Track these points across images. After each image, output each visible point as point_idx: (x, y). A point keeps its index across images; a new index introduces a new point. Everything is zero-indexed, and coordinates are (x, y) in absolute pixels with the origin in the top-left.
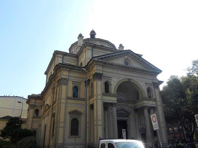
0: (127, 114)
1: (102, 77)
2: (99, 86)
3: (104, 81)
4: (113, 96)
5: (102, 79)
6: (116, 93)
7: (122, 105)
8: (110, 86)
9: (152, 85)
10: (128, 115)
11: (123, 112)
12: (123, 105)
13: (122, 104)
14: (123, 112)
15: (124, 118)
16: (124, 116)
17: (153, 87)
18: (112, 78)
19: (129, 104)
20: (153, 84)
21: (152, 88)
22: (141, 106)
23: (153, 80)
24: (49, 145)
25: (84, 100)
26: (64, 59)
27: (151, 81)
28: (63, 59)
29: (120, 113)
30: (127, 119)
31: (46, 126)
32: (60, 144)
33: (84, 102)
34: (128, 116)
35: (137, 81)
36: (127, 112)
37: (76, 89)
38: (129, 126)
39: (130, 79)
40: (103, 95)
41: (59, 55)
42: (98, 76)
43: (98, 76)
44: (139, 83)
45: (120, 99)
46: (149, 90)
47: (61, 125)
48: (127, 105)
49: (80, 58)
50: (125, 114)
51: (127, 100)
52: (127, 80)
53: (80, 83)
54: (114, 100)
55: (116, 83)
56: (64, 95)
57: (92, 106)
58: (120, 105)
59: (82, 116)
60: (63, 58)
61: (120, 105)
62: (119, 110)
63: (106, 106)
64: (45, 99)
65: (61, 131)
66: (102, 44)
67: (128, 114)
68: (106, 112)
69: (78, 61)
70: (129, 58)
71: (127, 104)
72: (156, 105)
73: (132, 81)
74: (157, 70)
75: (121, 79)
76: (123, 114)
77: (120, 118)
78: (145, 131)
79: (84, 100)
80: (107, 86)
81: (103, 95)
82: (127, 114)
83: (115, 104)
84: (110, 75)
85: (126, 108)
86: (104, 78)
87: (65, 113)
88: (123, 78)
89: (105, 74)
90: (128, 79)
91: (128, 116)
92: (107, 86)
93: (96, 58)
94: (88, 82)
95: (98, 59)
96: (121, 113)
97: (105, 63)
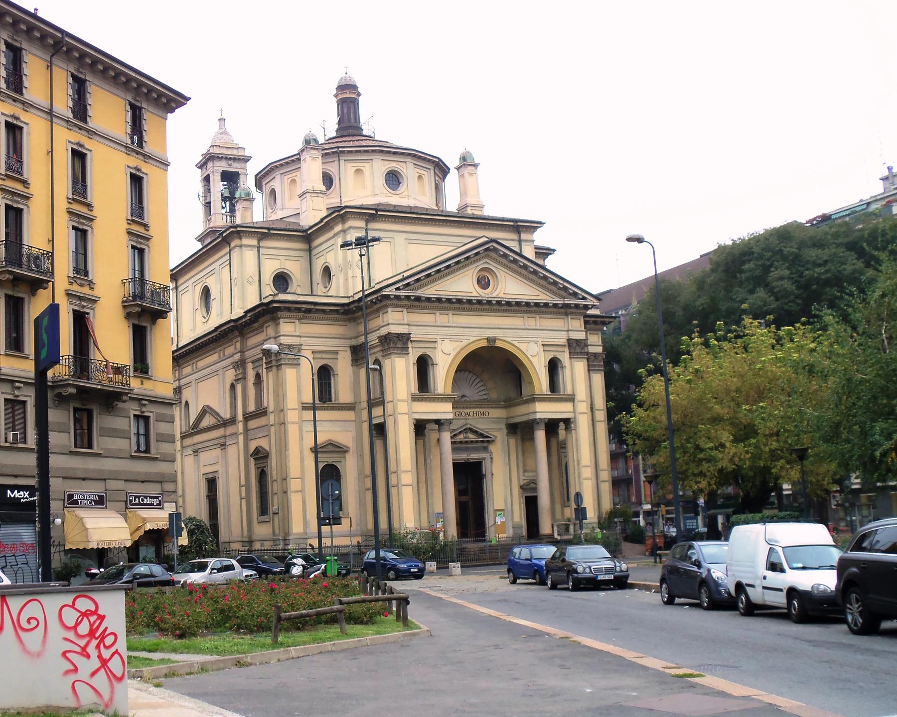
0: (482, 442)
1: (410, 345)
2: (400, 372)
3: (414, 353)
5: (410, 349)
6: (449, 391)
8: (431, 367)
9: (567, 350)
12: (471, 414)
13: (468, 411)
14: (472, 437)
15: (474, 456)
16: (476, 450)
18: (439, 341)
19: (490, 410)
20: (570, 346)
21: (564, 357)
22: (525, 418)
23: (568, 331)
24: (250, 537)
25: (350, 407)
26: (262, 251)
27: (564, 335)
28: (259, 251)
29: (461, 442)
30: (484, 459)
31: (212, 483)
32: (297, 534)
33: (350, 415)
34: (485, 449)
35: (516, 343)
36: (482, 435)
37: (324, 374)
38: (488, 476)
39: (494, 340)
40: (414, 398)
41: (245, 241)
42: (397, 343)
43: (397, 343)
44: (523, 347)
45: (463, 396)
46: (553, 366)
47: (294, 485)
48: (484, 414)
49: (318, 246)
50: (477, 442)
51: (485, 397)
52: (485, 344)
53: (336, 352)
54: (444, 410)
55: (451, 357)
56: (292, 401)
57: (379, 430)
59: (347, 455)
60: (259, 247)
61: (461, 414)
62: (460, 432)
63: (420, 427)
64: (183, 382)
65: (295, 501)
66: (394, 164)
67: (488, 441)
68: (420, 442)
69: (310, 254)
70: (492, 265)
71: (485, 410)
72: (574, 412)
73: (499, 344)
74: (584, 298)
75: (465, 342)
76: (472, 442)
77: (463, 456)
78: (535, 489)
79: (350, 407)
80: (423, 365)
81: (414, 398)
82: (485, 441)
83: (449, 422)
85: (480, 425)
86: (414, 344)
87: (301, 451)
88: (472, 339)
89: (417, 333)
90: (488, 340)
91: (485, 449)
92: (423, 365)
93: (388, 289)
94: (358, 353)
95: (397, 289)
96: (466, 442)
97: (418, 299)
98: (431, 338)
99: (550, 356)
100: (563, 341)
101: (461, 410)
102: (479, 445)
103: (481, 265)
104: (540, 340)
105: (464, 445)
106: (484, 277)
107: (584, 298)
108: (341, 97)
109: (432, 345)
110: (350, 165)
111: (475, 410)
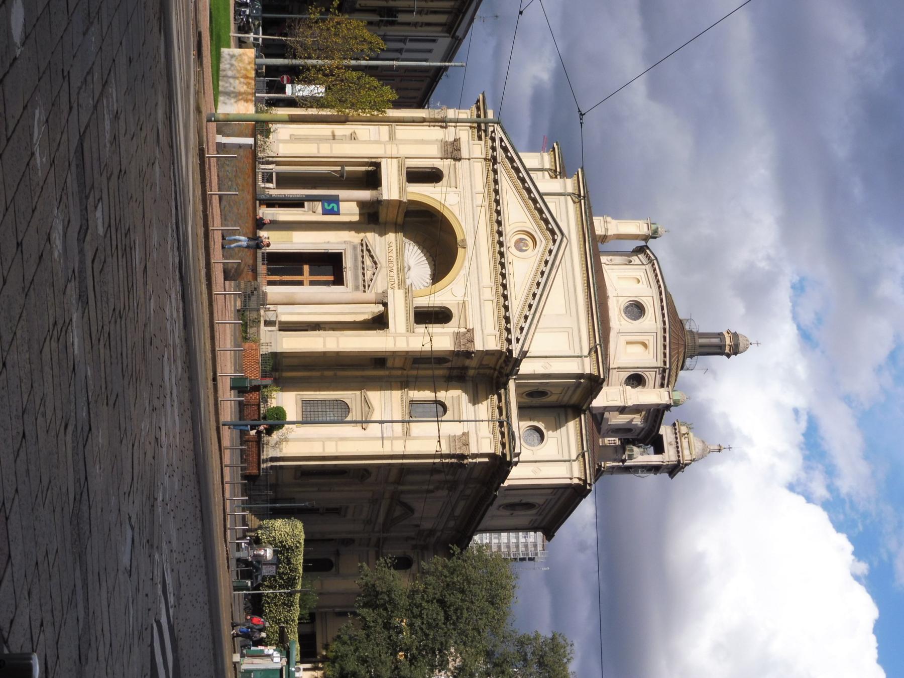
0: (364, 281)
3: (443, 165)
4: (402, 190)
7: (391, 271)
9: (463, 330)
10: (361, 288)
11: (368, 274)
12: (392, 274)
13: (395, 270)
15: (348, 275)
16: (356, 277)
17: (456, 330)
29: (363, 263)
35: (463, 272)
52: (459, 237)
58: (392, 262)
61: (391, 262)
73: (460, 251)
76: (364, 274)
80: (432, 176)
84: (464, 182)
88: (463, 224)
90: (464, 240)
91: (357, 288)
92: (432, 176)
96: (363, 268)
98: (460, 184)
99: (454, 311)
100: (470, 326)
101: (395, 263)
102: (361, 282)
103: (538, 235)
104: (469, 300)
105: (360, 265)
106: (527, 245)
107: (518, 340)
108: (726, 335)
109: (453, 184)
110: (642, 274)
111: (396, 278)
